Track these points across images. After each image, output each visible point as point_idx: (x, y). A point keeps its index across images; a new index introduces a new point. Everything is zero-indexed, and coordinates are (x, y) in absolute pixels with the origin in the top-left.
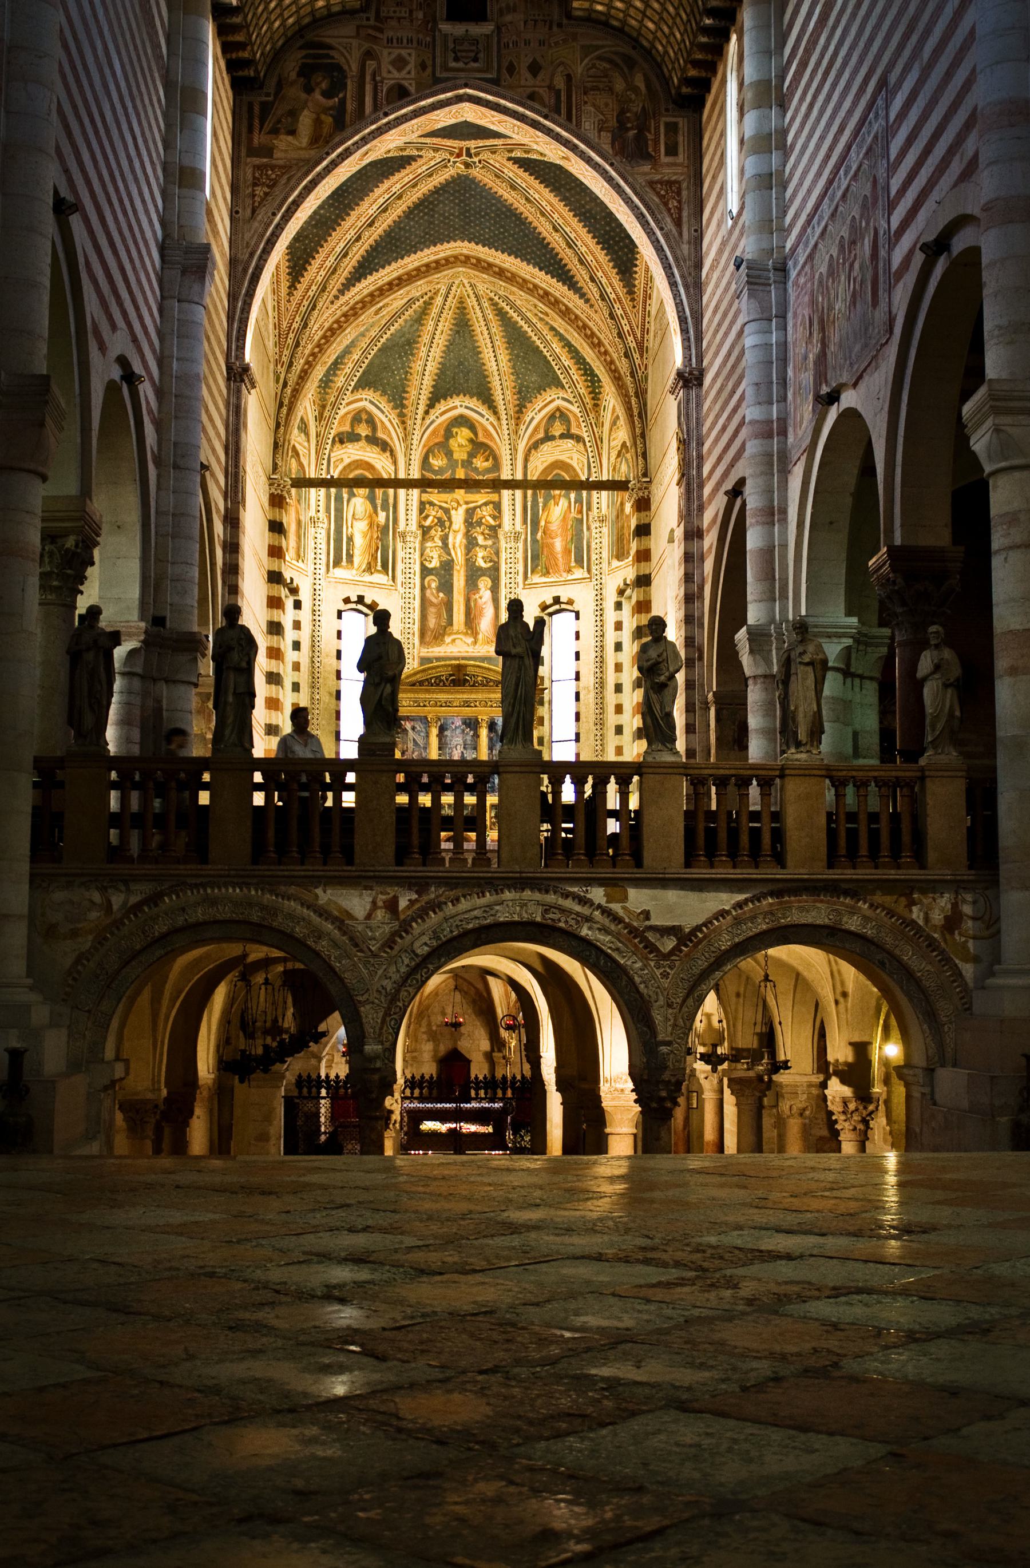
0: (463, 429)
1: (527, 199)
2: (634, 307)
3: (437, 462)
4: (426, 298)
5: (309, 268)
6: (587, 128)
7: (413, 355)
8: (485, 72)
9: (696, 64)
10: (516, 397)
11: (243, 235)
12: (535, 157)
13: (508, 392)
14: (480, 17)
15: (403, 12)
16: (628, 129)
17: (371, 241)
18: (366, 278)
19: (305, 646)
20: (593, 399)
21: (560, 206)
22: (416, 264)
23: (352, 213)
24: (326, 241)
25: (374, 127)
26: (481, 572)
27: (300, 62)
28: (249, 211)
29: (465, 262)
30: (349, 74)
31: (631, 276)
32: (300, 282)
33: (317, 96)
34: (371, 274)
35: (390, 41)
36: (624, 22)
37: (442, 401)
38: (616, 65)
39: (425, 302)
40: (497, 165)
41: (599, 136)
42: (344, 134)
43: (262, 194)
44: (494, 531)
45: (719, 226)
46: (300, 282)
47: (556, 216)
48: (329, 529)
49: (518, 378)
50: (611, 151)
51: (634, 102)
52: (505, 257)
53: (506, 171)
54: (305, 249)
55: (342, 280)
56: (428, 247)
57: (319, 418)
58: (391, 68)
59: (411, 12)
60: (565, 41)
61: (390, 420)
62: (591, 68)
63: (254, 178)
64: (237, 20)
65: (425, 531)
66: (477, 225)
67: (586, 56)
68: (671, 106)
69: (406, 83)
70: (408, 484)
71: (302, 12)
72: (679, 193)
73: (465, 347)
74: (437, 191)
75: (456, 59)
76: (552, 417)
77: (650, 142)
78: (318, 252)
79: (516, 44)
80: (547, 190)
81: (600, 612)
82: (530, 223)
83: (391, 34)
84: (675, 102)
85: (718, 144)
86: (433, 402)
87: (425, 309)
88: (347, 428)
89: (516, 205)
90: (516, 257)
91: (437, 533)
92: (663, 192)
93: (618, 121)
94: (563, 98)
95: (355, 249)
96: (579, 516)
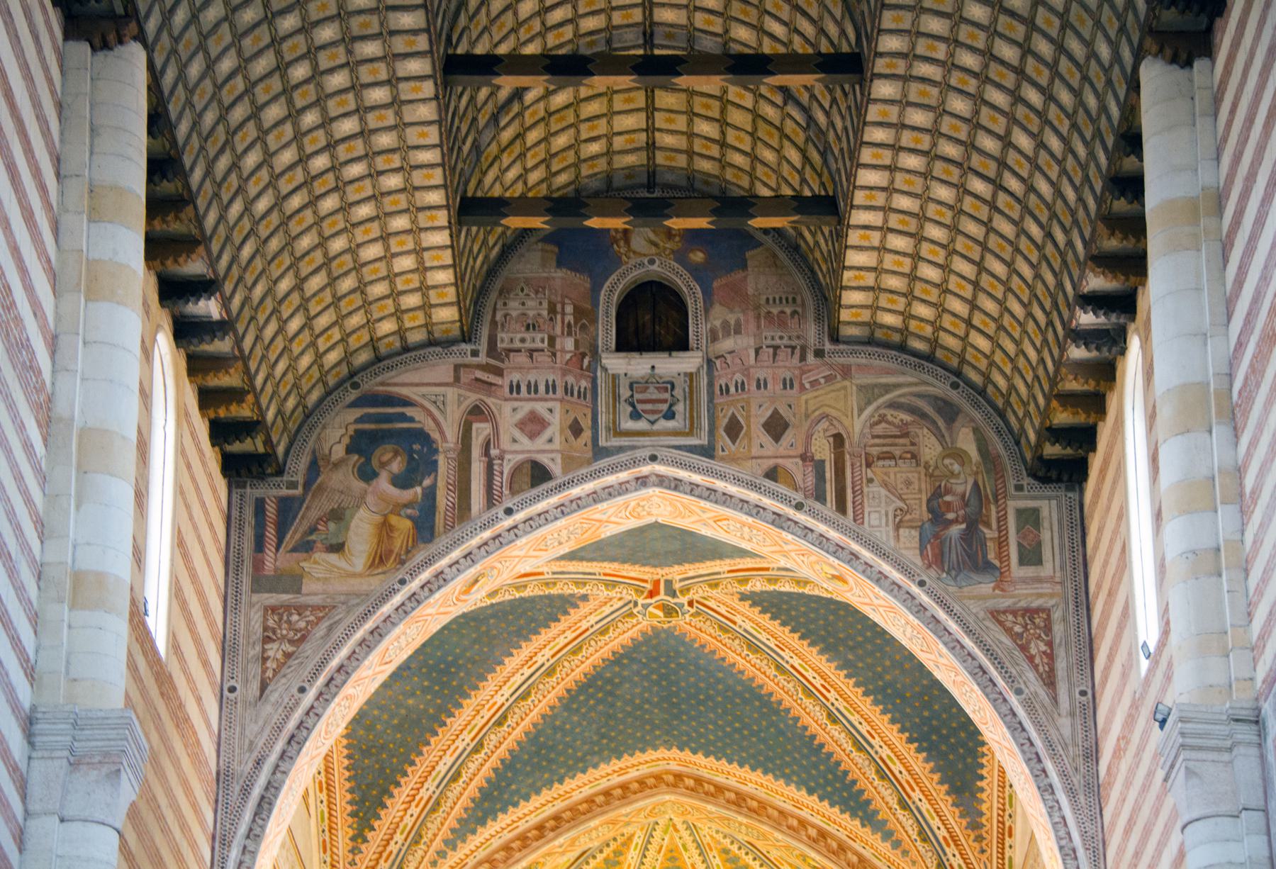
1: (779, 667)
2: (983, 851)
4: (607, 851)
5: (388, 803)
6: (875, 522)
8: (690, 434)
9: (1068, 399)
11: (243, 728)
12: (787, 588)
15: (538, 340)
16: (952, 522)
17: (502, 751)
18: (495, 819)
21: (839, 678)
22: (587, 791)
23: (465, 702)
24: (420, 753)
25: (487, 534)
27: (352, 429)
28: (255, 686)
29: (675, 786)
30: (442, 446)
31: (973, 796)
32: (373, 829)
34: (504, 810)
35: (515, 388)
36: (934, 343)
38: (923, 416)
39: (606, 860)
40: (723, 610)
41: (897, 538)
42: (433, 548)
43: (280, 655)
45: (1125, 676)
46: (373, 829)
47: (832, 695)
50: (918, 561)
51: (957, 476)
52: (745, 772)
53: (738, 619)
54: (382, 769)
55: (451, 822)
56: (607, 760)
58: (517, 434)
59: (552, 340)
60: (829, 379)
62: (877, 423)
63: (266, 629)
64: (223, 346)
66: (691, 718)
67: (869, 403)
68: (1026, 481)
69: (544, 459)
71: (354, 342)
72: (1048, 629)
74: (618, 659)
75: (636, 415)
77: (989, 544)
78: (405, 774)
79: (741, 387)
80: (815, 650)
82: (788, 710)
83: (515, 377)
84: (1033, 474)
85: (1116, 532)
89: (761, 678)
90: (765, 772)
92: (1018, 629)
93: (930, 510)
94: (829, 474)
95: (473, 767)
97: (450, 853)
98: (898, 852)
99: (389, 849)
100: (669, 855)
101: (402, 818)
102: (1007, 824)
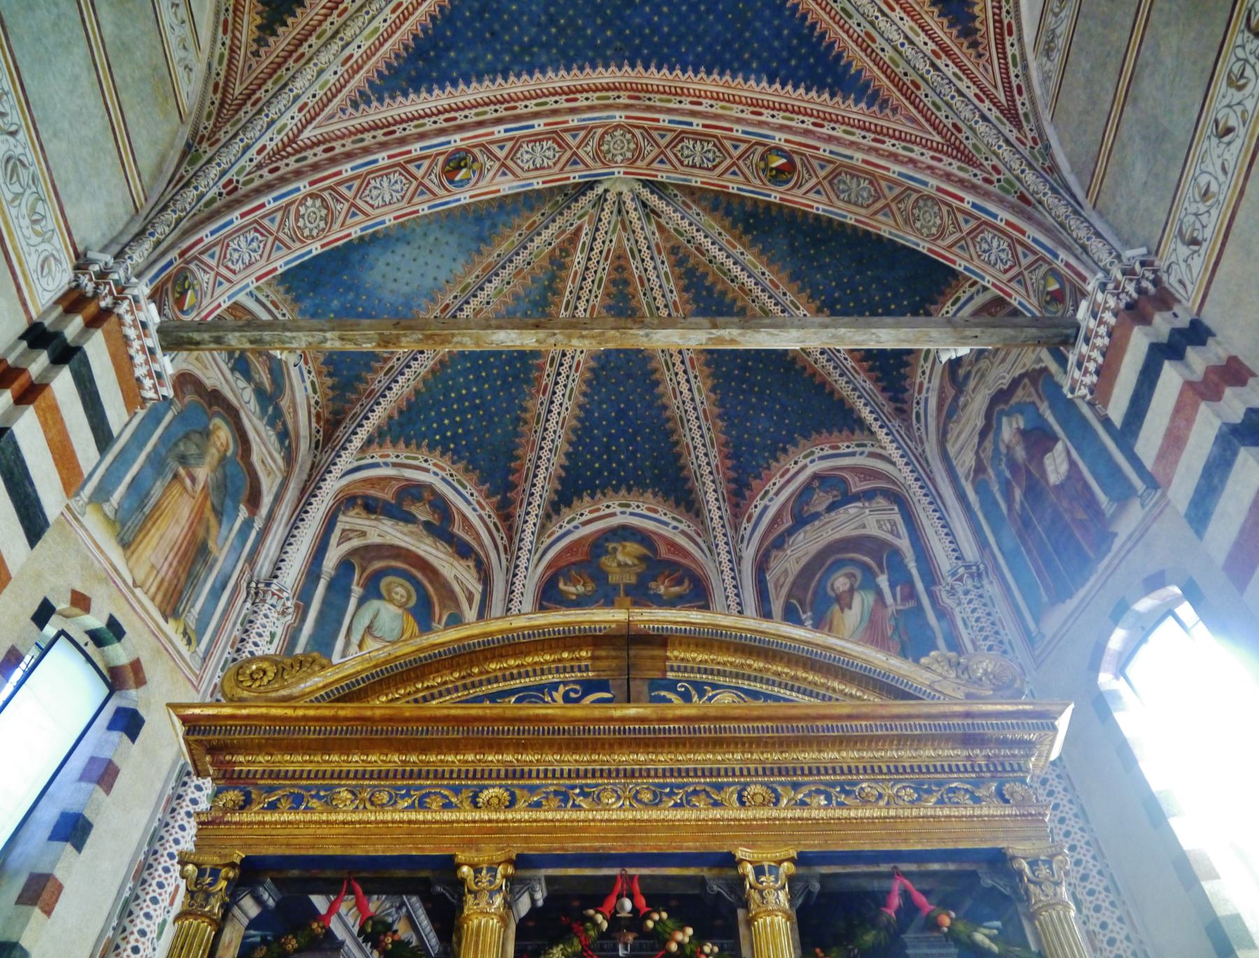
0: (628, 544)
2: (980, 56)
7: (528, 381)
10: (729, 463)
13: (713, 452)
20: (891, 399)
37: (587, 499)
48: (299, 630)
49: (731, 426)
61: (480, 517)
73: (629, 375)
87: (553, 278)
88: (388, 495)
96: (911, 604)
97: (375, 104)
98: (875, 108)
99: (301, 50)
100: (617, 263)
101: (320, 22)
102: (1006, 22)
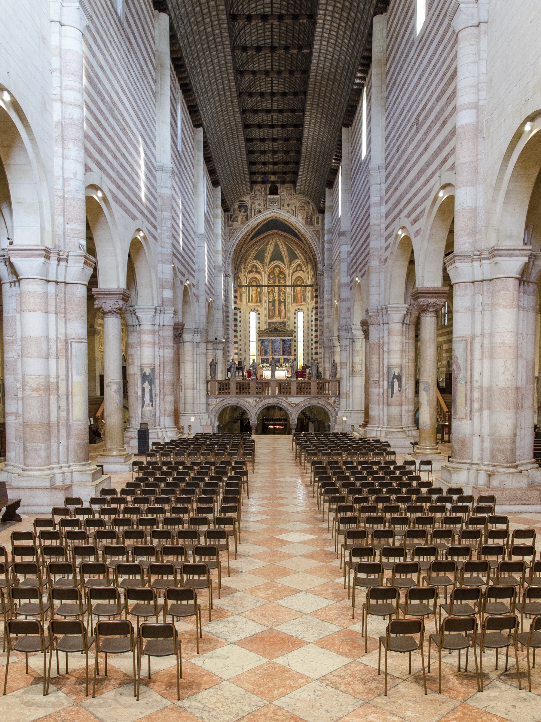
3: (271, 276)
14: (277, 194)
19: (242, 321)
26: (282, 302)
33: (242, 213)
44: (284, 293)
57: (244, 268)
65: (269, 293)
70: (265, 286)
76: (297, 266)
81: (308, 312)
86: (271, 261)
91: (272, 293)
